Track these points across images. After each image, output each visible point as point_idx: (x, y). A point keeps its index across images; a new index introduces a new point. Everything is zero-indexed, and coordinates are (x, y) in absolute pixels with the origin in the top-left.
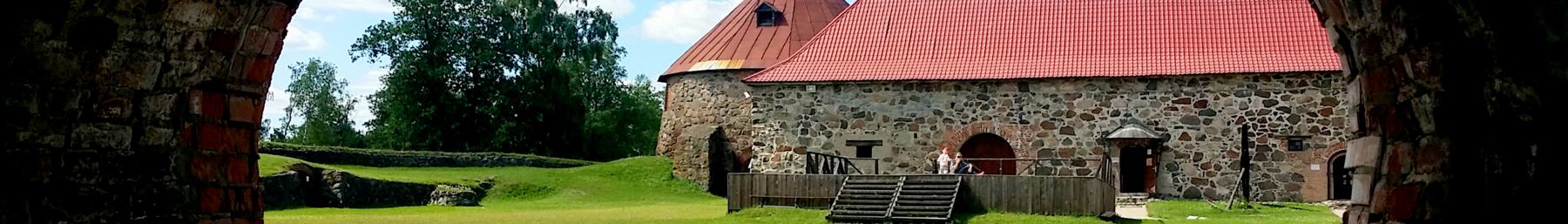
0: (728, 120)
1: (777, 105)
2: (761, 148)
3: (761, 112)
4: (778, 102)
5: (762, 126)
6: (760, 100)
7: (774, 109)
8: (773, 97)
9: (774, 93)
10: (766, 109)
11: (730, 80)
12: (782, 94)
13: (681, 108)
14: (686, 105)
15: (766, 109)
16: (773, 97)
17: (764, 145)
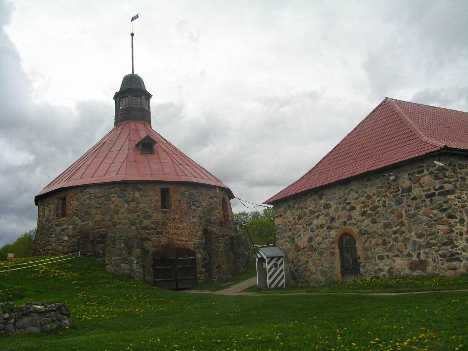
0: (141, 222)
1: (460, 176)
2: (455, 220)
3: (450, 183)
4: (461, 174)
5: (452, 197)
6: (447, 170)
7: (460, 180)
8: (457, 168)
9: (457, 163)
10: (453, 180)
11: (139, 190)
12: (462, 165)
13: (88, 213)
14: (94, 211)
15: (453, 180)
16: (457, 168)
17: (456, 218)
